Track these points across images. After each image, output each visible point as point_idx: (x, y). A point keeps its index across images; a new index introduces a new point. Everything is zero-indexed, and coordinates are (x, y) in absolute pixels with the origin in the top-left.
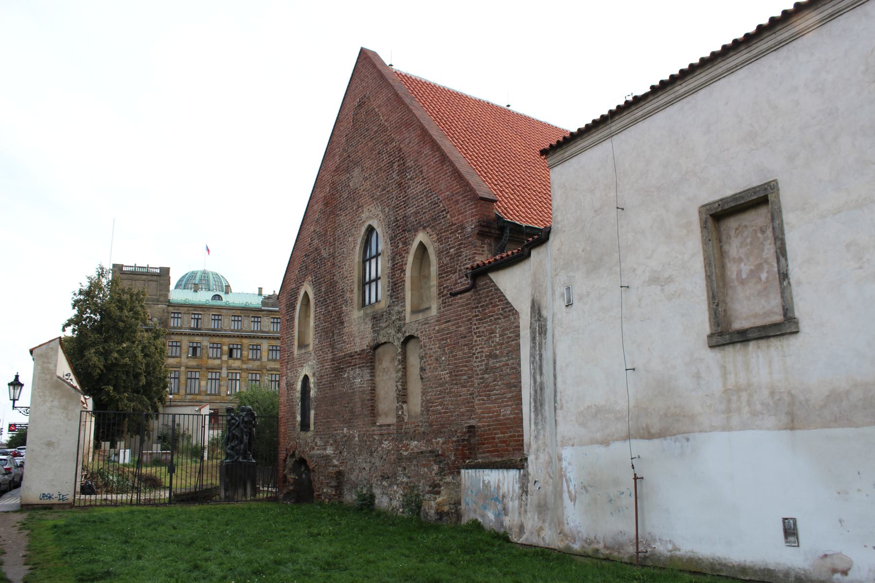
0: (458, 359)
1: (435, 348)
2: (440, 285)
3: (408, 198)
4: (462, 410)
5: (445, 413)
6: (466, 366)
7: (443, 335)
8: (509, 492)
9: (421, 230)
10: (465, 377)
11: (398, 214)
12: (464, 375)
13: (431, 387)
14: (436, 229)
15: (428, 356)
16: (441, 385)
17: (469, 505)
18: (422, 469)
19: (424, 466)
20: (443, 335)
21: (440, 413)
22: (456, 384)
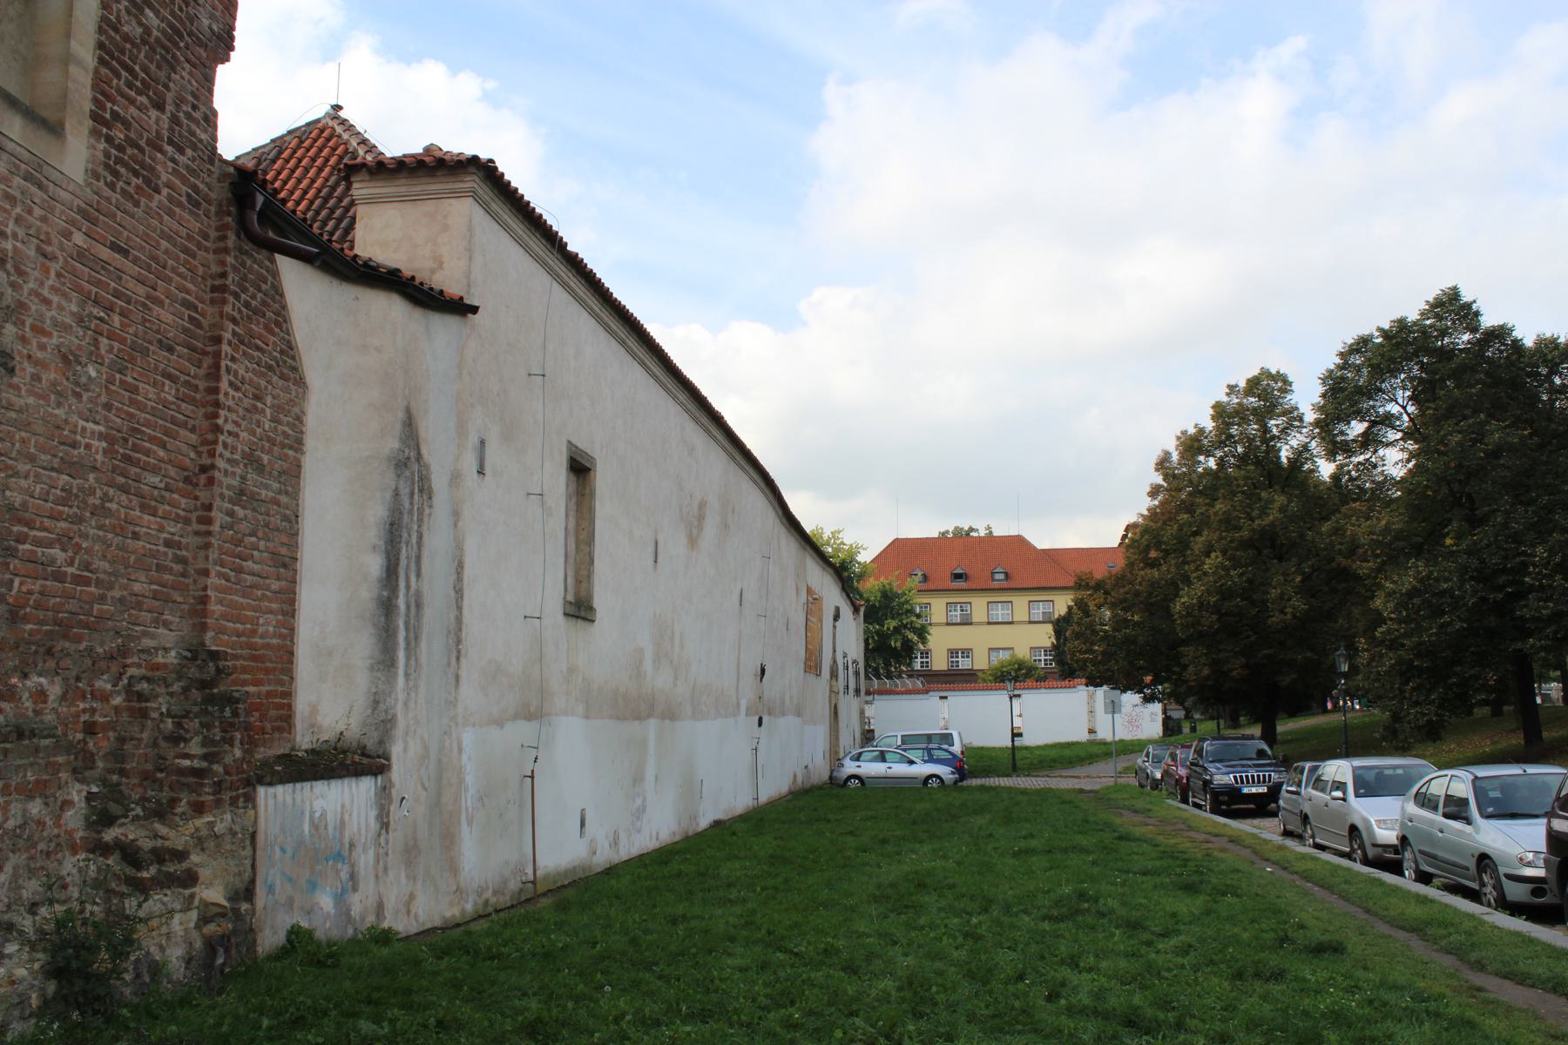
0: (141, 408)
1: (61, 308)
4: (137, 587)
5: (79, 580)
6: (163, 446)
7: (98, 283)
8: (359, 830)
10: (155, 480)
12: (155, 470)
13: (32, 459)
15: (29, 322)
16: (73, 468)
17: (273, 894)
18: (16, 808)
19: (28, 793)
20: (98, 283)
21: (59, 577)
22: (124, 489)
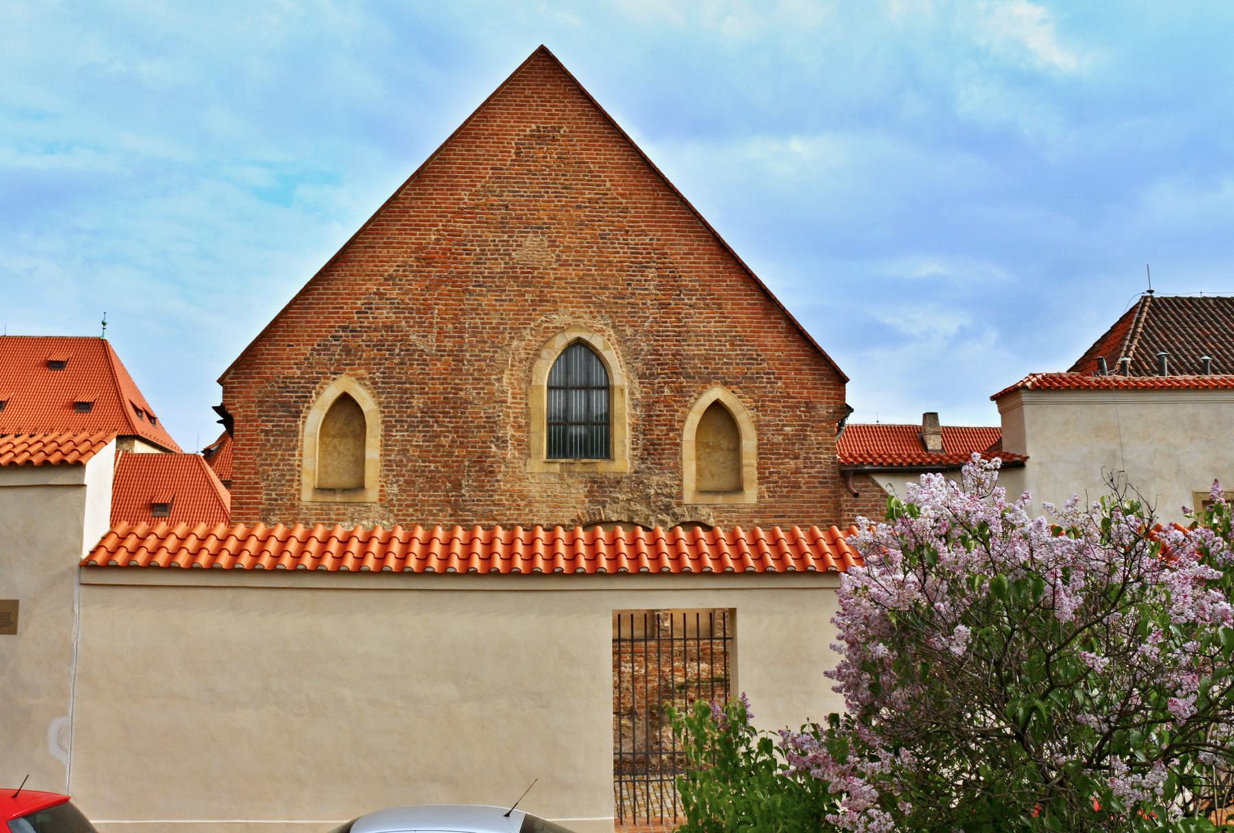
2: (761, 468)
3: (688, 332)
9: (716, 383)
11: (662, 346)
14: (754, 392)
